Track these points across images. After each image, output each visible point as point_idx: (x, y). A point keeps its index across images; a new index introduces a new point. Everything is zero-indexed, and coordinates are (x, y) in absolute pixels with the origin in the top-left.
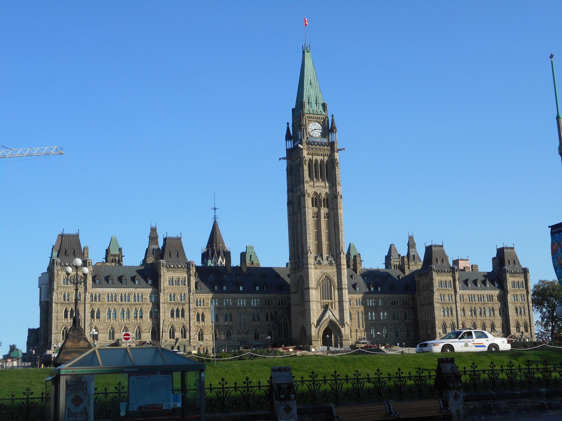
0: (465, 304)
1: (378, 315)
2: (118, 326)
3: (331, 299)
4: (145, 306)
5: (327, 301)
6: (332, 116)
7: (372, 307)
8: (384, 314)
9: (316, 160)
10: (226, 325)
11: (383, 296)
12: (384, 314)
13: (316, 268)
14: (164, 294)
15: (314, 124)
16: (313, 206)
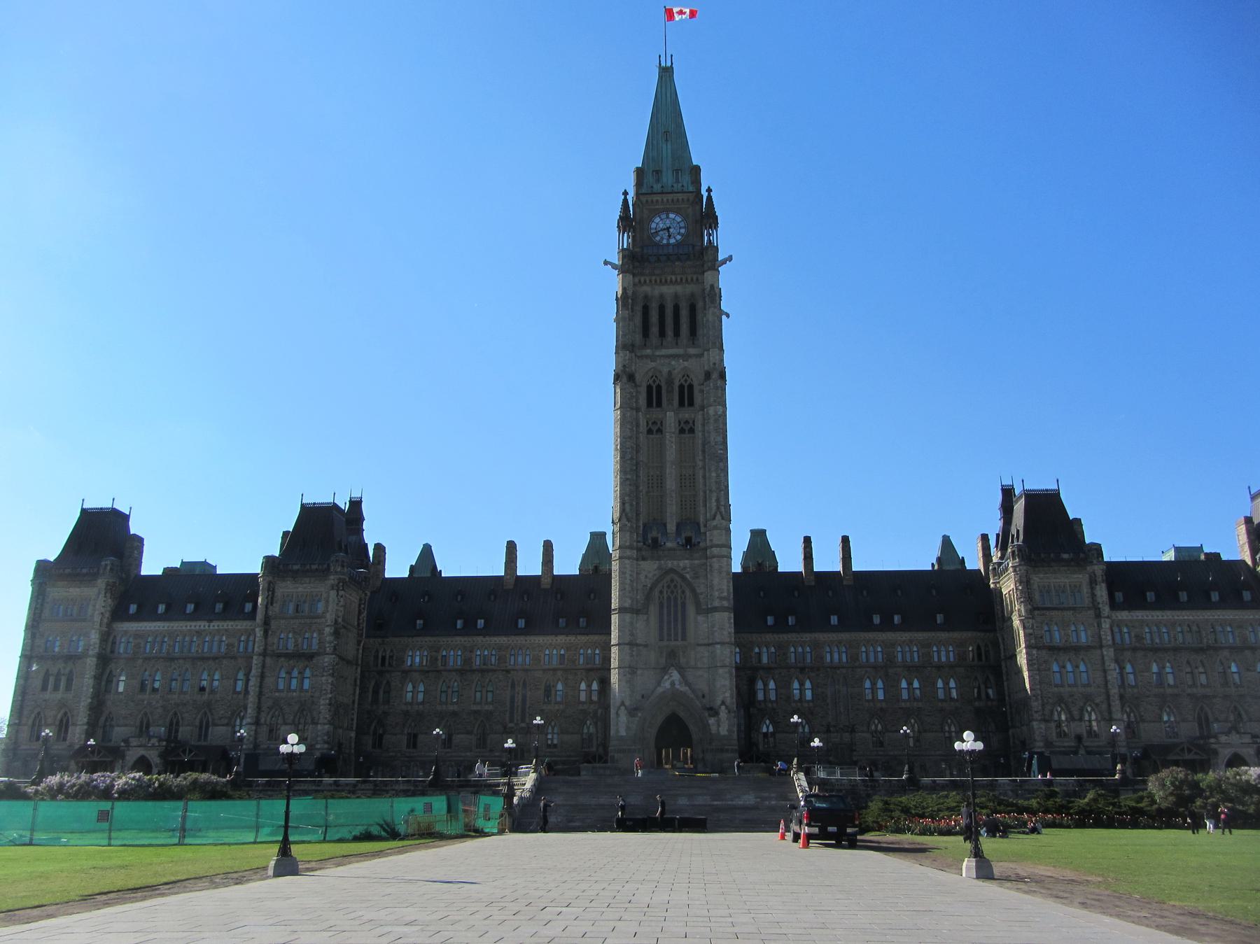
0: (1134, 649)
1: (892, 685)
2: (160, 710)
3: (684, 638)
4: (225, 662)
5: (673, 643)
6: (709, 190)
7: (875, 667)
8: (910, 684)
9: (662, 296)
10: (476, 712)
11: (906, 636)
12: (910, 684)
13: (644, 559)
14: (266, 632)
15: (664, 216)
16: (649, 404)
